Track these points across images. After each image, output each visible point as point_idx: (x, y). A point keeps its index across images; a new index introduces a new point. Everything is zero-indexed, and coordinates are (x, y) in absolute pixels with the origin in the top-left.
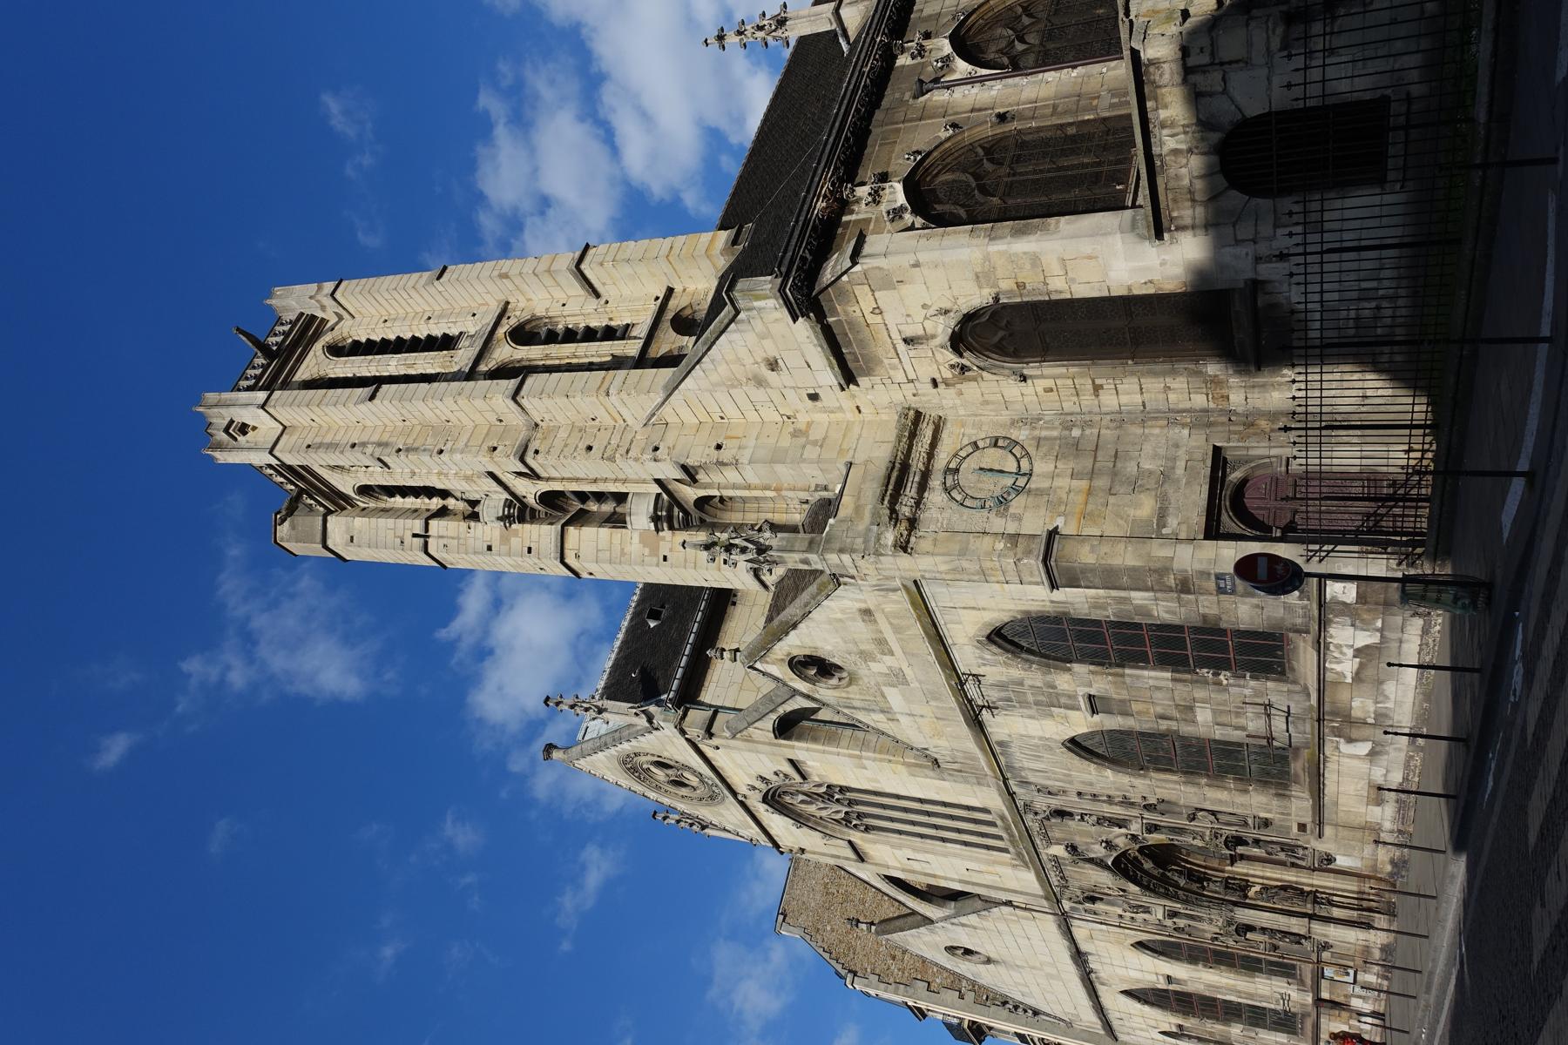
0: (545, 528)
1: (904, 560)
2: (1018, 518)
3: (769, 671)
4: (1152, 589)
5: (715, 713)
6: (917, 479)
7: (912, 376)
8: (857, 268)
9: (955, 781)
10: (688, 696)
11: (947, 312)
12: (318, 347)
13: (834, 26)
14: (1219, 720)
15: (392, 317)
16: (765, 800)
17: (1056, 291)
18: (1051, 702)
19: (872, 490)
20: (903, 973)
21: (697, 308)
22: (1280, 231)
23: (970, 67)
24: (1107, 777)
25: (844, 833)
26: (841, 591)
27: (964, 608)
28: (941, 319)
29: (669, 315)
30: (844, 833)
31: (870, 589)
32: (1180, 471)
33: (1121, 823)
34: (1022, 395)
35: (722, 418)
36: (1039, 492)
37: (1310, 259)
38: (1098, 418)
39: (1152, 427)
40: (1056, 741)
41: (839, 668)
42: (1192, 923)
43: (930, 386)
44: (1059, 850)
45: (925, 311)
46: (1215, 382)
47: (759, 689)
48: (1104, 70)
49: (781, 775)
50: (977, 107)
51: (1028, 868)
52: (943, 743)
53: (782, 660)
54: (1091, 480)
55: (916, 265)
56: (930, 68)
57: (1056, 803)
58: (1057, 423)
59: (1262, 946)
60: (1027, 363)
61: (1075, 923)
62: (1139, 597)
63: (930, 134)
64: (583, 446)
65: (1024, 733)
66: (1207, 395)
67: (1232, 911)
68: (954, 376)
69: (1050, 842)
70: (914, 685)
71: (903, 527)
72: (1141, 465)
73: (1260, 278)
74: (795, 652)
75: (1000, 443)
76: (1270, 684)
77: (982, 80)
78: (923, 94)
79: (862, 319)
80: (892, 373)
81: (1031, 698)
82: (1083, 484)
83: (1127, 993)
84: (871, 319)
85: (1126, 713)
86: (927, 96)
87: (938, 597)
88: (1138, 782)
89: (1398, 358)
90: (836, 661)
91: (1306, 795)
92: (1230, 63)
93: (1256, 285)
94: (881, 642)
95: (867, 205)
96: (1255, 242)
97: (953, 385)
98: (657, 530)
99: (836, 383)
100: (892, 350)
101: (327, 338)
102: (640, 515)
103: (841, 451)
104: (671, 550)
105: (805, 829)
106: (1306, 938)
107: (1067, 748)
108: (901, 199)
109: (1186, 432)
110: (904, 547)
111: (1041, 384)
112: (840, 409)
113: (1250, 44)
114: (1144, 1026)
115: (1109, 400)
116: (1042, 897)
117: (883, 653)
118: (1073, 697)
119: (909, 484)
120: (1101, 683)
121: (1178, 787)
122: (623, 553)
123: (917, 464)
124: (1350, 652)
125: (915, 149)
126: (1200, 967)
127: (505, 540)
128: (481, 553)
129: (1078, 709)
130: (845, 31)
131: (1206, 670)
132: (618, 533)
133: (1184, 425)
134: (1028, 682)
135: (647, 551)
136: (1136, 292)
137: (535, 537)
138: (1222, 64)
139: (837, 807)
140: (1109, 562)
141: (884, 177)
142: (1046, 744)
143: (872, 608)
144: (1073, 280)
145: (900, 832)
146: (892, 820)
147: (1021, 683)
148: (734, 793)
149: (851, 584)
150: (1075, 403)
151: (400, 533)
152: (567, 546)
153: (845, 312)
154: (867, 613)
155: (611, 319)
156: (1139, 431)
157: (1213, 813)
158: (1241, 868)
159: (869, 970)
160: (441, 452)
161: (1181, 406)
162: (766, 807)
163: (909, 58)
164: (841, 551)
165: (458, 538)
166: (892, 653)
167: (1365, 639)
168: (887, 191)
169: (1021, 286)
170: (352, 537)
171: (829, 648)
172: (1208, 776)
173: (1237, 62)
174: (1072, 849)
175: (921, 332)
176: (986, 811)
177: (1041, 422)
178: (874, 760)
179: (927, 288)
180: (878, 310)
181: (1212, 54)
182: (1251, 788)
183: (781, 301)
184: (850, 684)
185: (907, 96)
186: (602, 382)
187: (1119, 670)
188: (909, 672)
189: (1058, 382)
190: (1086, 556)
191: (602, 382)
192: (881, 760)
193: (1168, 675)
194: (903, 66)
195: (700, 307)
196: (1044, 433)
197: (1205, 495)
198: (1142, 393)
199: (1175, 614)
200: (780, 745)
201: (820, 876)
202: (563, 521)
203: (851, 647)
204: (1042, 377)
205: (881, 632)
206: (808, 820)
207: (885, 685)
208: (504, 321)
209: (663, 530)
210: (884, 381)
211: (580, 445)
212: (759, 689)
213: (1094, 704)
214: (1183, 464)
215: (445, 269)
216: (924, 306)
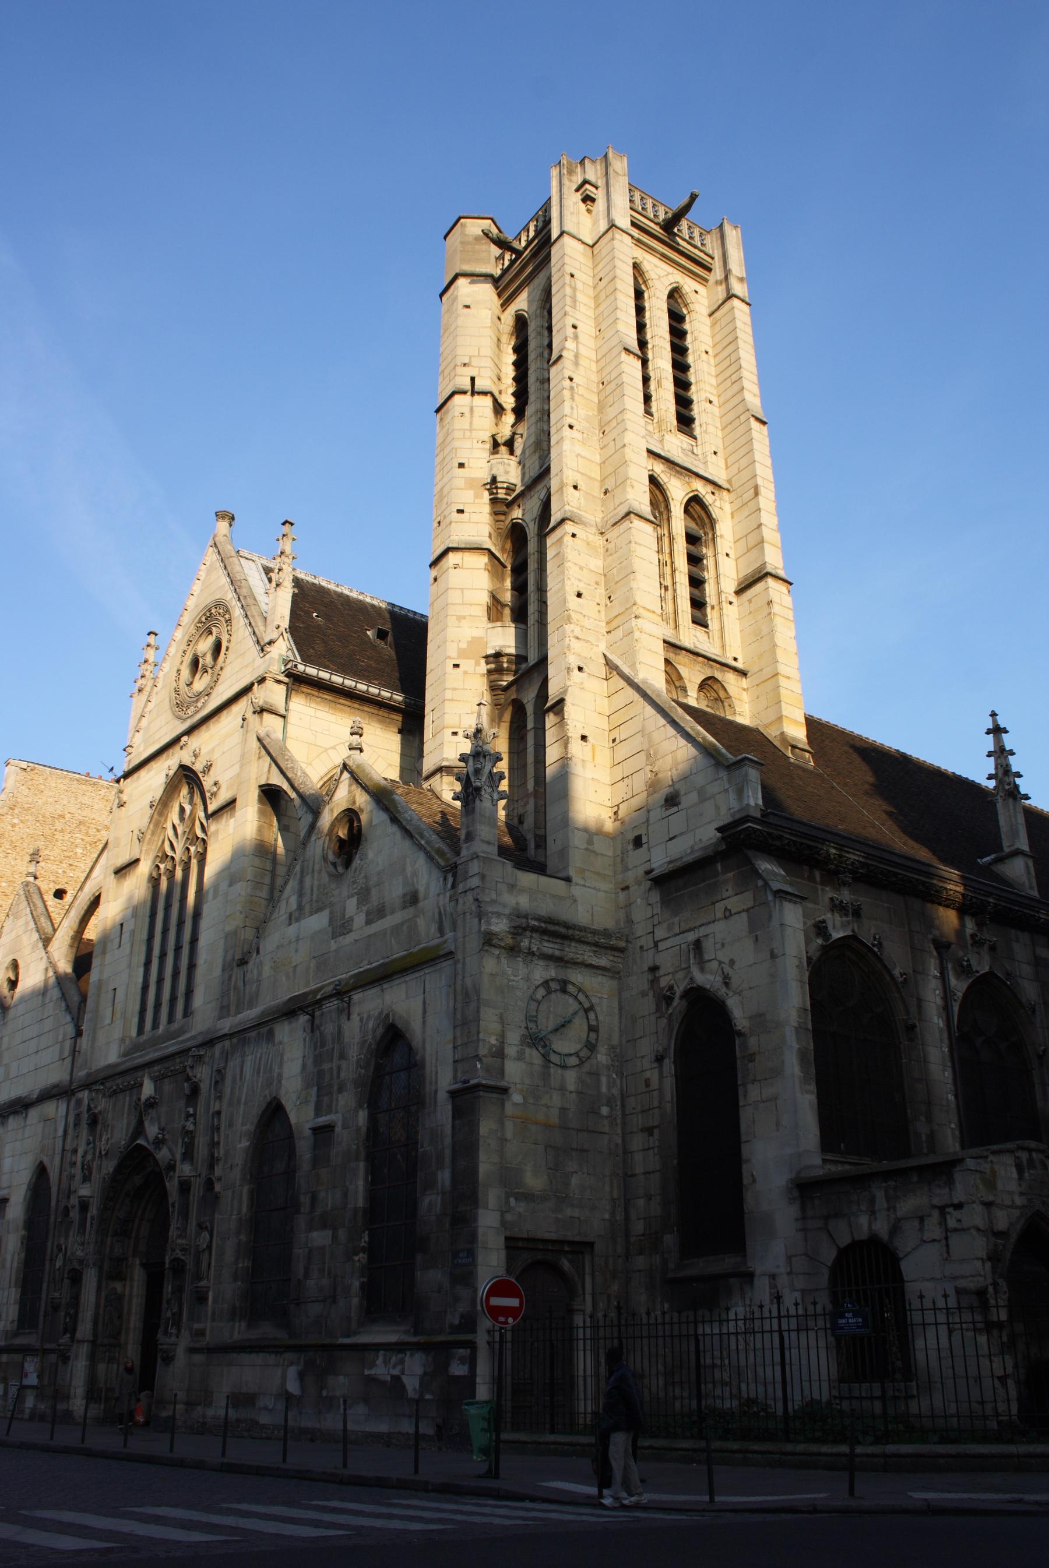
1: (473, 943)
2: (520, 1057)
3: (341, 786)
5: (284, 717)
6: (557, 953)
7: (662, 946)
8: (770, 897)
9: (223, 983)
11: (727, 985)
12: (677, 277)
13: (1007, 850)
16: (183, 767)
17: (746, 1091)
19: (546, 908)
21: (726, 704)
22: (798, 1294)
23: (960, 995)
24: (240, 1142)
26: (436, 874)
27: (424, 1003)
28: (719, 979)
29: (718, 675)
31: (441, 903)
32: (569, 1212)
33: (188, 1155)
34: (643, 1057)
35: (614, 740)
36: (545, 1076)
37: (775, 1321)
38: (619, 1131)
41: (348, 864)
42: (76, 1224)
43: (651, 964)
44: (148, 1089)
45: (727, 962)
47: (311, 764)
48: (953, 1126)
49: (215, 789)
51: (125, 1055)
52: (267, 971)
53: (354, 802)
57: (204, 1087)
59: (57, 1295)
60: (675, 1062)
61: (63, 1106)
62: (445, 1177)
65: (285, 1058)
66: (643, 1235)
67: (94, 1265)
68: (662, 989)
69: (157, 1080)
70: (333, 945)
71: (509, 941)
72: (575, 1175)
73: (756, 1280)
75: (593, 1035)
76: (355, 1301)
77: (947, 1008)
78: (936, 948)
79: (720, 898)
80: (665, 925)
81: (326, 1066)
82: (555, 1120)
84: (720, 907)
85: (316, 1162)
86: (935, 953)
88: (236, 1174)
89: (678, 1404)
90: (357, 862)
91: (236, 1336)
92: (947, 1246)
93: (749, 1277)
94: (380, 912)
95: (832, 899)
96: (789, 1273)
97: (652, 987)
98: (486, 657)
99: (654, 866)
100: (688, 927)
101: (689, 285)
103: (582, 871)
104: (465, 673)
105: (150, 812)
106: (72, 1338)
107: (269, 1104)
108: (836, 935)
109: (607, 1216)
111: (654, 1076)
112: (626, 869)
115: (638, 1142)
117: (368, 914)
119: (552, 945)
121: (235, 1212)
123: (573, 951)
124: (396, 1372)
125: (885, 943)
127: (470, 483)
130: (1000, 860)
131: (367, 1239)
132: (481, 612)
133: (613, 1213)
134: (344, 1064)
135: (464, 645)
136: (745, 1167)
137: (475, 518)
138: (946, 1238)
139: (179, 847)
140: (481, 1149)
141: (857, 913)
143: (421, 905)
147: (342, 1056)
148: (189, 732)
149: (445, 884)
150: (634, 1109)
154: (412, 899)
155: (713, 607)
157: (209, 1247)
158: (138, 1275)
162: (175, 768)
163: (971, 932)
165: (471, 430)
166: (369, 922)
167: (411, 1384)
168: (845, 919)
169: (751, 1058)
170: (468, 307)
171: (371, 854)
173: (948, 1252)
174: (151, 1104)
175: (707, 957)
176: (187, 1012)
177: (614, 1076)
179: (750, 966)
180: (728, 914)
181: (955, 1230)
182: (239, 1283)
183: (738, 816)
184: (330, 875)
186: (649, 610)
188: (349, 939)
189: (656, 1094)
190: (486, 1127)
191: (649, 610)
193: (361, 1204)
195: (727, 708)
196: (604, 1079)
197: (547, 1236)
198: (644, 1173)
201: (72, 810)
202: (493, 550)
204: (661, 1077)
205: (392, 913)
206: (161, 814)
207: (331, 913)
208: (710, 488)
209: (487, 663)
210: (656, 917)
212: (311, 764)
213: (323, 1133)
214: (576, 1215)
215: (764, 423)
216: (732, 962)
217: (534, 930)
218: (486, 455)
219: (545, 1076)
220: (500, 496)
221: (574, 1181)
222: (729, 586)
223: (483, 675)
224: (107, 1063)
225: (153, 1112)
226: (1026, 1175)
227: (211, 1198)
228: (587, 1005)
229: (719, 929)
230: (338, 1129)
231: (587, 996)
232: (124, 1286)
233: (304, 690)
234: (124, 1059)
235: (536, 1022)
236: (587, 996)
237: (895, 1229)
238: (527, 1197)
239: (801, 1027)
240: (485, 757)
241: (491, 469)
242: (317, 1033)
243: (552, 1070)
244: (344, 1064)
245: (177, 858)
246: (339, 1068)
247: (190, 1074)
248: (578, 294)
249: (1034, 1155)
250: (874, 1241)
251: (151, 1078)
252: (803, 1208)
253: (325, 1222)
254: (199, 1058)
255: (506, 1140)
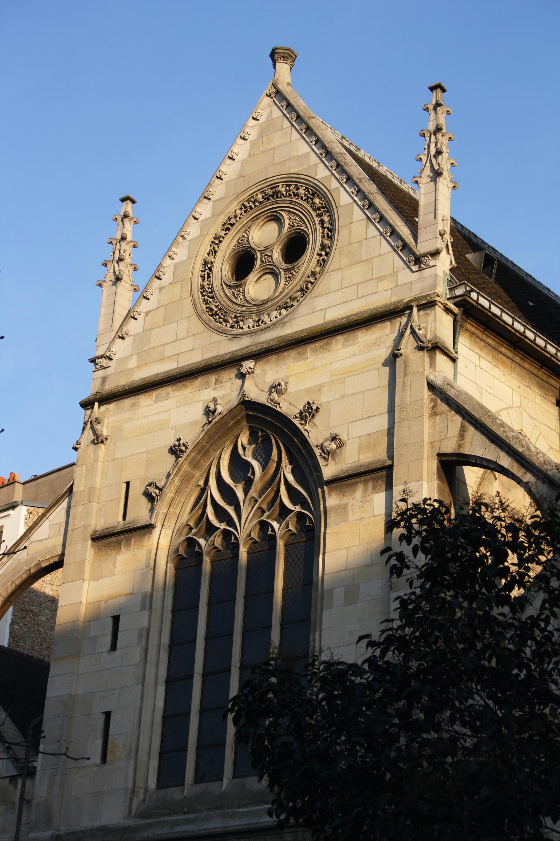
224: (96, 824)
233: (469, 327)
234: (140, 822)
245: (242, 535)
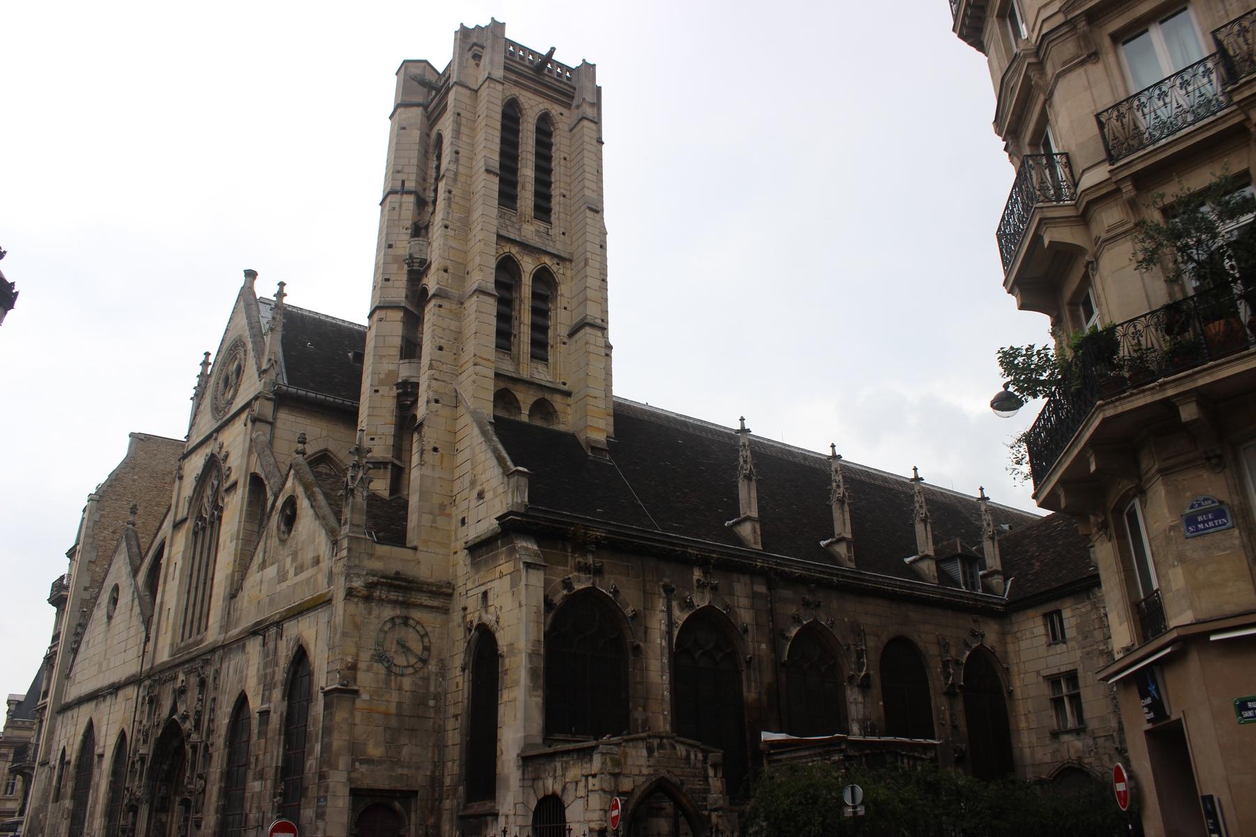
0: (403, 293)
2: (369, 669)
4: (321, 756)
5: (271, 424)
10: (282, 400)
11: (497, 622)
12: (545, 105)
14: (255, 796)
15: (569, 165)
16: (213, 455)
18: (267, 685)
19: (393, 567)
20: (102, 541)
22: (518, 828)
23: (681, 623)
25: (193, 514)
28: (494, 618)
29: (548, 397)
30: (193, 514)
32: (400, 771)
33: (197, 726)
39: (433, 753)
40: (245, 685)
46: (455, 790)
48: (666, 713)
49: (228, 473)
50: (649, 631)
52: (245, 604)
53: (294, 491)
54: (397, 715)
55: (520, 606)
56: (687, 593)
58: (439, 690)
62: (318, 747)
63: (630, 602)
64: (443, 342)
67: (147, 802)
69: (187, 673)
71: (365, 592)
74: (298, 502)
75: (426, 653)
80: (471, 580)
83: (90, 726)
85: (259, 733)
86: (664, 595)
87: (322, 615)
90: (293, 532)
93: (496, 815)
94: (300, 569)
95: (579, 562)
96: (515, 815)
97: (463, 622)
101: (555, 110)
102: (405, 371)
104: (382, 396)
109: (429, 773)
110: (350, 593)
111: (460, 680)
113: (594, 811)
114: (68, 735)
115: (451, 724)
116: (153, 664)
117: (296, 569)
118: (269, 701)
120: (275, 720)
122: (381, 357)
125: (621, 591)
126: (110, 778)
127: (396, 259)
128: (387, 240)
129: (262, 704)
131: (283, 787)
132: (396, 352)
133: (433, 772)
134: (277, 669)
135: (382, 376)
136: (498, 744)
137: (397, 284)
142: (243, 679)
143: (321, 565)
144: (506, 706)
145: (193, 558)
146: (201, 553)
147: (277, 665)
149: (333, 552)
151: (406, 170)
152: (389, 311)
153: (502, 553)
156: (431, 744)
159: (103, 512)
160: (446, 227)
161: (445, 769)
163: (697, 577)
164: (349, 550)
166: (296, 575)
169: (506, 672)
172: (225, 787)
175: (490, 603)
177: (441, 679)
178: (236, 550)
181: (592, 791)
185: (666, 580)
186: (485, 359)
187: (283, 733)
188: (284, 585)
191: (485, 359)
192: (235, 555)
193: (280, 764)
194: (693, 574)
197: (382, 787)
198: (453, 745)
199: (310, 770)
200: (246, 477)
202: (408, 307)
203: (299, 548)
205: (307, 569)
207: (279, 566)
209: (397, 389)
211: (444, 340)
213: (265, 714)
217: (382, 584)
218: (408, 237)
219: (388, 682)
220: (415, 268)
221: (405, 751)
222: (563, 331)
223: (394, 397)
225: (183, 697)
226: (656, 754)
227: (208, 757)
228: (422, 633)
229: (496, 584)
230: (272, 713)
231: (423, 627)
232: (167, 816)
235: (383, 646)
236: (423, 627)
237: (564, 789)
238: (370, 761)
239: (533, 653)
240: (359, 467)
241: (410, 249)
242: (266, 648)
243: (393, 678)
244: (277, 669)
246: (274, 672)
247: (201, 672)
248: (462, 128)
249: (665, 741)
250: (554, 795)
251: (184, 673)
252: (523, 773)
253: (261, 776)
254: (207, 662)
255: (355, 724)
